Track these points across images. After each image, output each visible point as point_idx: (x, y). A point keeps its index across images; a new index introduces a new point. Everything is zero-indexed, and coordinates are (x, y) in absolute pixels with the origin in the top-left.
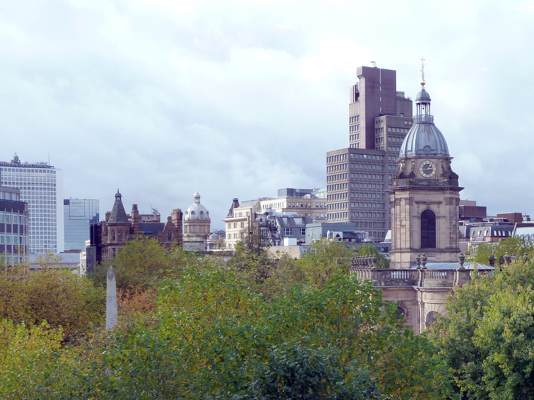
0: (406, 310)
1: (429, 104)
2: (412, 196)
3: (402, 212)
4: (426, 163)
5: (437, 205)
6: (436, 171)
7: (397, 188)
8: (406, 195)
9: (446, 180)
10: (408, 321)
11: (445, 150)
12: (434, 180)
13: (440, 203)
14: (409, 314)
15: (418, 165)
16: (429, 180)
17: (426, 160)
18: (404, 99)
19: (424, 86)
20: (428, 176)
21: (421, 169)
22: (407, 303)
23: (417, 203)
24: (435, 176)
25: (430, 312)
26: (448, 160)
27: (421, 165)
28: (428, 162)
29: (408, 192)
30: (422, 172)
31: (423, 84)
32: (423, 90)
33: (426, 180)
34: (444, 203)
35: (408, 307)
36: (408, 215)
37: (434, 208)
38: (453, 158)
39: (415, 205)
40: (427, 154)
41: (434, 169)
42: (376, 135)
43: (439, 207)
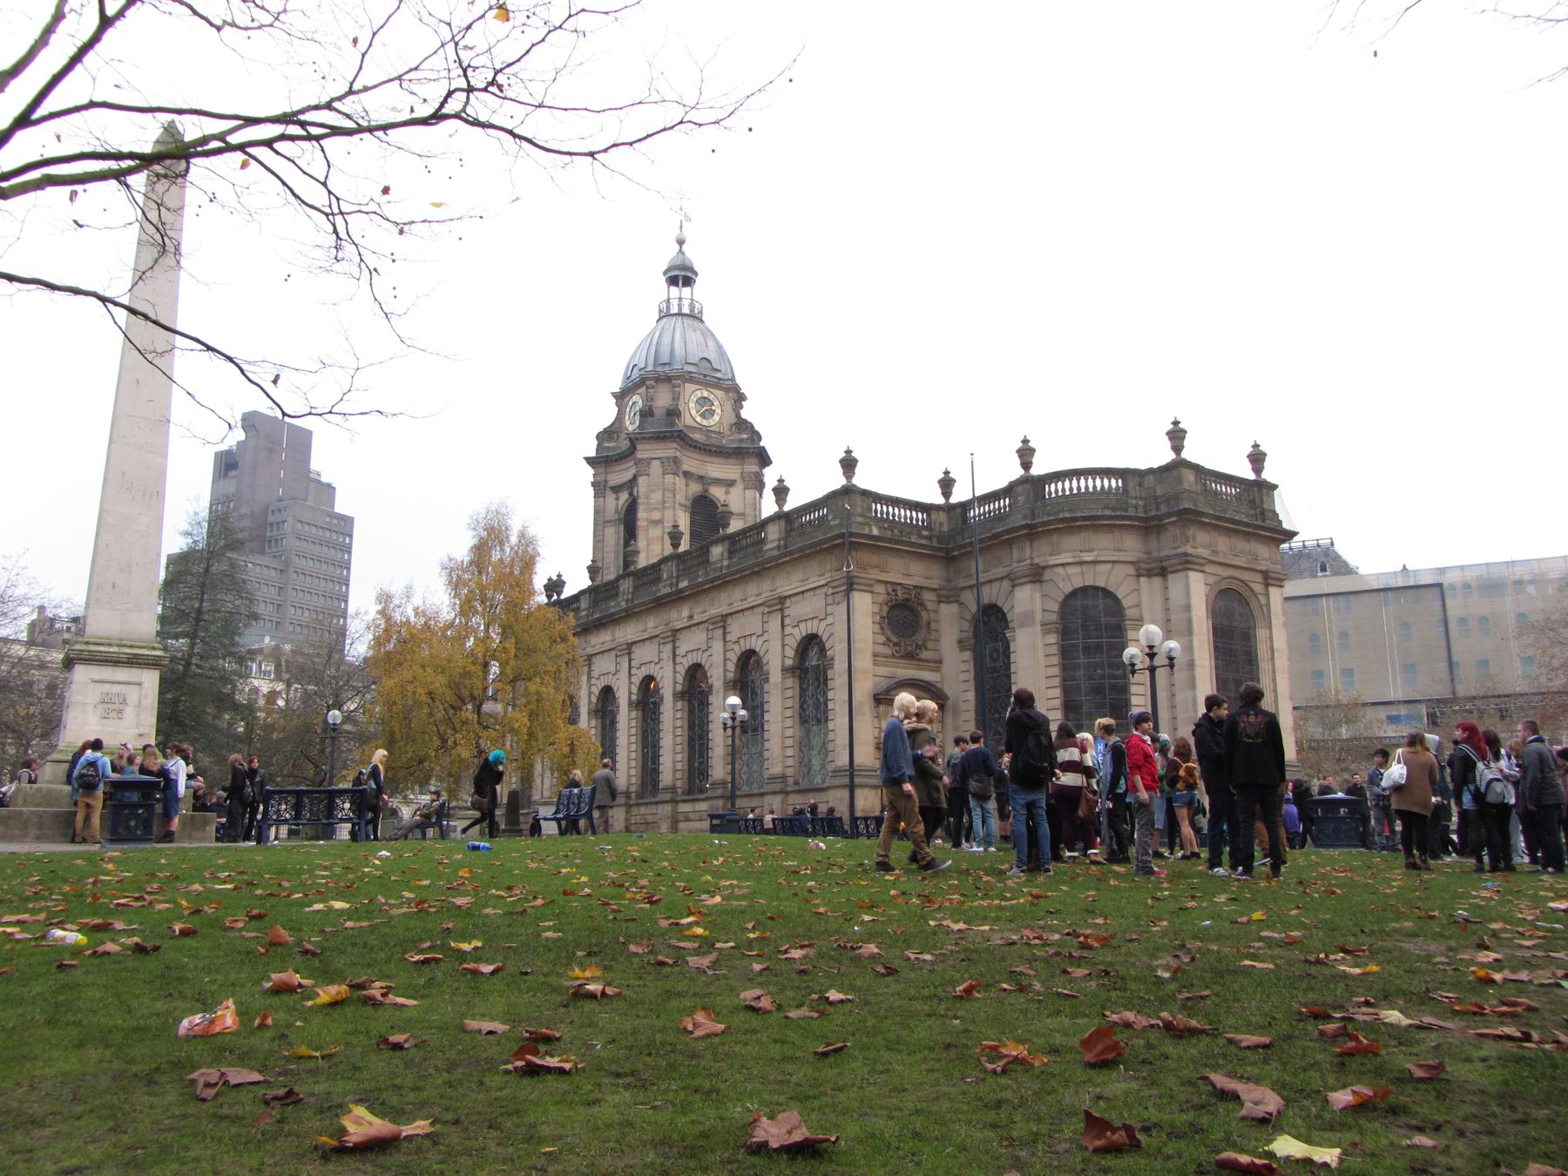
0: (924, 614)
2: (678, 454)
3: (652, 491)
6: (718, 418)
8: (669, 450)
9: (745, 436)
10: (930, 645)
11: (733, 379)
13: (730, 484)
14: (933, 625)
16: (707, 431)
18: (319, 482)
19: (684, 247)
20: (705, 423)
21: (692, 405)
22: (928, 597)
23: (687, 474)
25: (1074, 594)
26: (740, 398)
28: (706, 394)
29: (675, 445)
30: (693, 412)
33: (701, 429)
34: (740, 486)
35: (930, 606)
37: (717, 493)
40: (705, 376)
41: (718, 411)
42: (268, 534)
43: (727, 493)
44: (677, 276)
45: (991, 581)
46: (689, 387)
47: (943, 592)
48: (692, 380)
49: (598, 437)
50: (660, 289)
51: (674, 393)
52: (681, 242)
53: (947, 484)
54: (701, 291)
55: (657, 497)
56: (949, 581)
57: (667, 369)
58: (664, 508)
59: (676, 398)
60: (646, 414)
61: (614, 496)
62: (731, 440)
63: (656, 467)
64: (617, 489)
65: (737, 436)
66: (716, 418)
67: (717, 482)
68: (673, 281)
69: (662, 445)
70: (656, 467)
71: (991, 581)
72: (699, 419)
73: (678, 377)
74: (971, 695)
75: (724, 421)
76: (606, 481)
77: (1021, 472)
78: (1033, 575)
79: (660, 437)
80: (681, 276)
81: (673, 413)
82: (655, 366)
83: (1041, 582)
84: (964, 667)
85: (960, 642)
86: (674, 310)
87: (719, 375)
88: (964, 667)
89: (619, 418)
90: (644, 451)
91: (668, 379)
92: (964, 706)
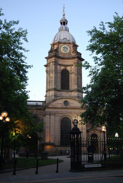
1: (67, 24)
13: (72, 65)
20: (65, 52)
23: (60, 65)
26: (75, 46)
28: (65, 46)
31: (64, 15)
32: (64, 17)
37: (68, 68)
38: (78, 46)
39: (58, 67)
44: (62, 22)
50: (59, 25)
54: (68, 25)
57: (56, 41)
59: (58, 48)
62: (73, 55)
66: (68, 51)
67: (67, 66)
68: (61, 23)
80: (64, 23)
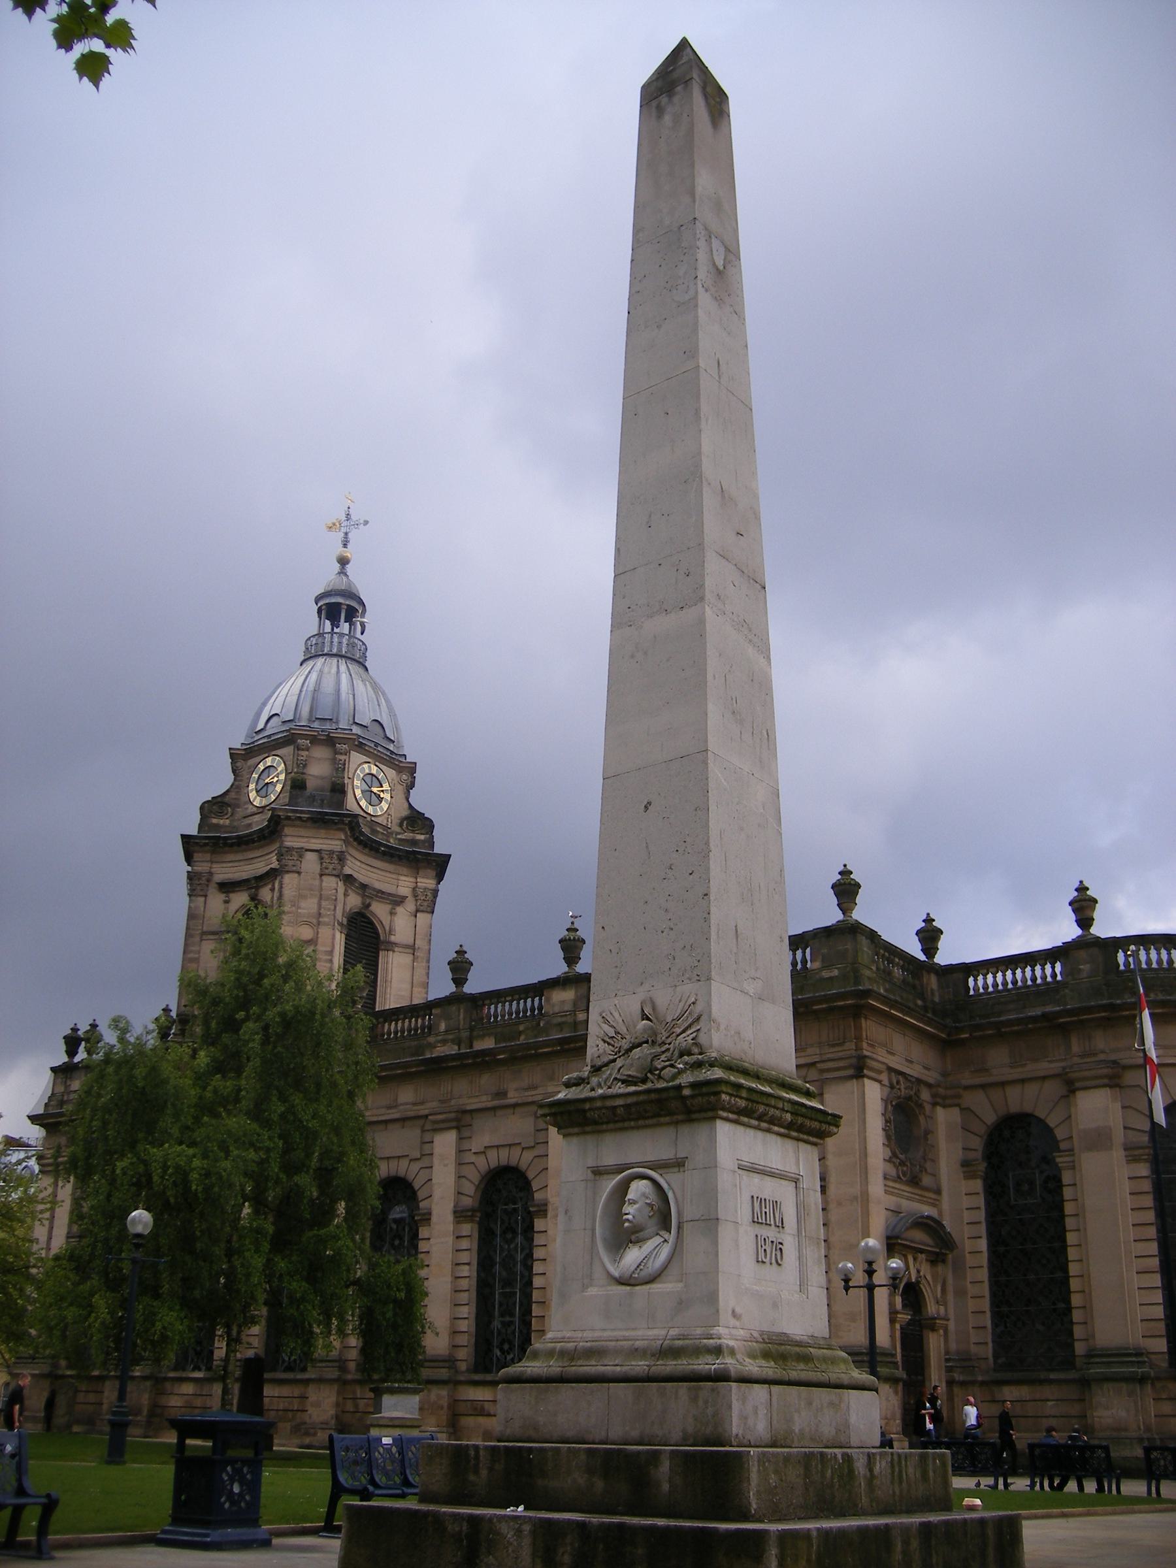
3: (304, 897)
4: (370, 767)
5: (390, 906)
7: (302, 812)
8: (334, 842)
12: (386, 827)
15: (352, 766)
17: (369, 760)
20: (370, 810)
21: (357, 783)
23: (349, 879)
24: (386, 815)
27: (358, 772)
28: (374, 770)
30: (358, 792)
36: (329, 909)
37: (379, 910)
40: (377, 744)
45: (1023, 1081)
46: (356, 757)
47: (941, 1091)
48: (360, 747)
49: (202, 808)
51: (334, 761)
52: (343, 562)
53: (930, 935)
55: (309, 906)
56: (945, 1074)
57: (327, 726)
58: (319, 923)
60: (297, 785)
61: (222, 897)
62: (399, 837)
63: (310, 862)
64: (227, 887)
65: (408, 835)
66: (385, 806)
67: (381, 895)
69: (323, 832)
70: (310, 862)
71: (1023, 1081)
72: (363, 803)
73: (344, 741)
74: (983, 1244)
75: (392, 813)
76: (211, 874)
77: (1079, 932)
78: (1111, 1077)
79: (320, 821)
81: (339, 790)
82: (310, 720)
83: (1118, 1086)
84: (967, 1202)
85: (965, 1164)
86: (335, 651)
87: (391, 747)
88: (967, 1202)
89: (238, 786)
90: (293, 839)
91: (330, 741)
92: (970, 1261)
